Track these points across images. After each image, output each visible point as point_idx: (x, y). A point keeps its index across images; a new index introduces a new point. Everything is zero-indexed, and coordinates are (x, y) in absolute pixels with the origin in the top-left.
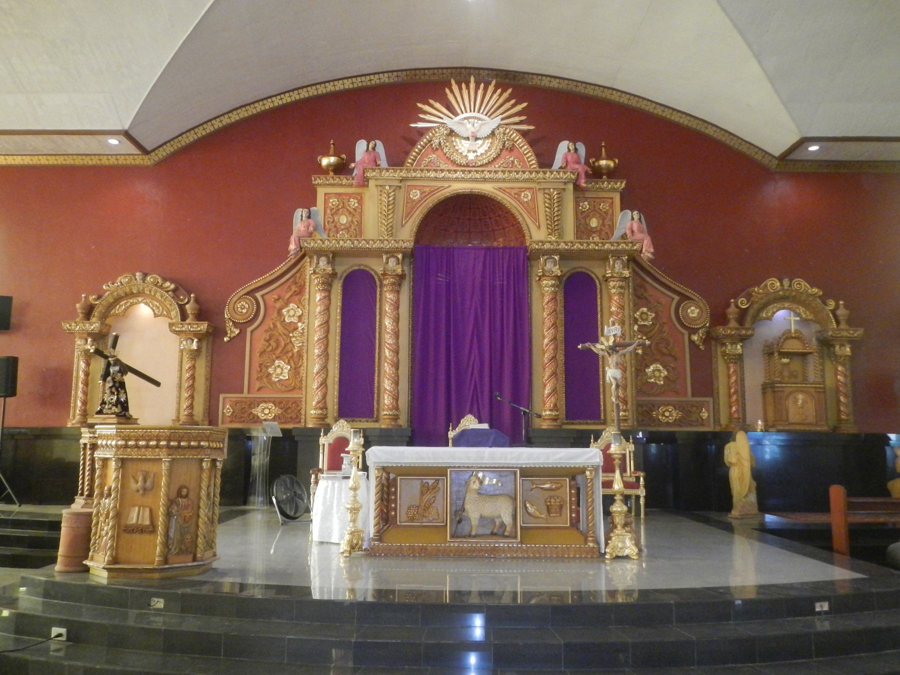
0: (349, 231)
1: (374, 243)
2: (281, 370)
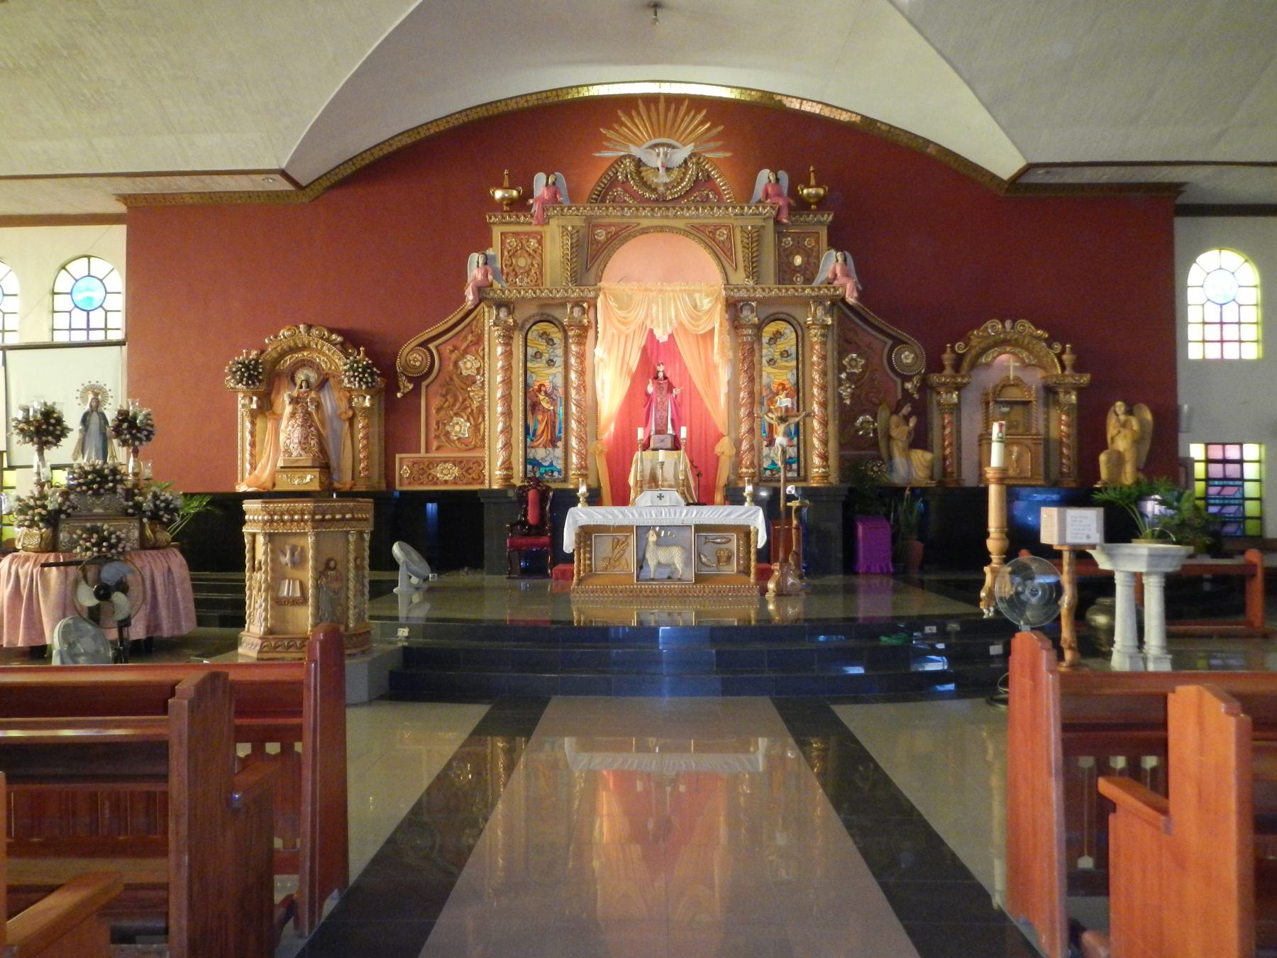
0: (528, 275)
2: (461, 427)
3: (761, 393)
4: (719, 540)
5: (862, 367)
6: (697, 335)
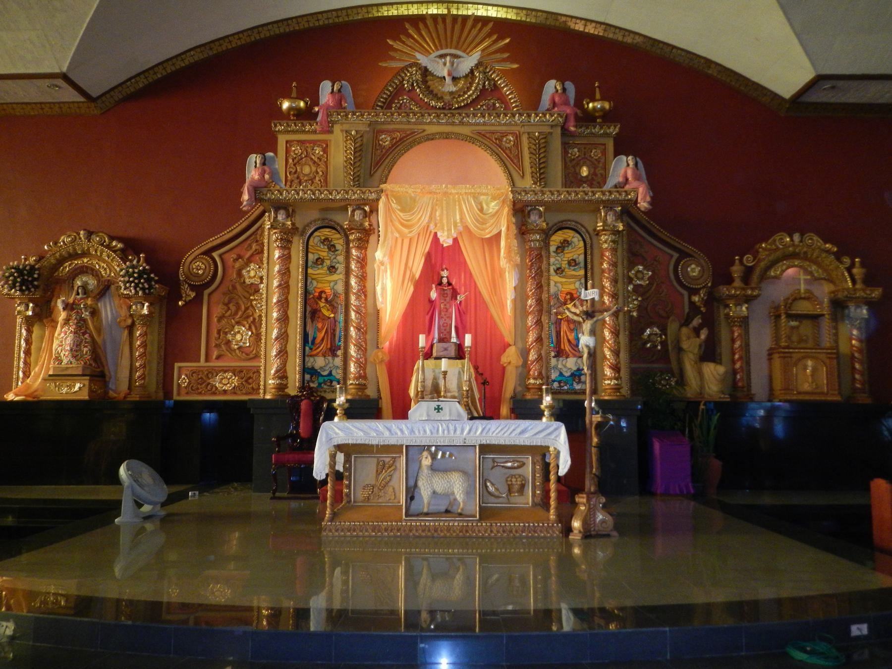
0: (313, 182)
1: (338, 193)
2: (242, 336)
3: (549, 302)
4: (509, 464)
5: (650, 278)
6: (482, 239)
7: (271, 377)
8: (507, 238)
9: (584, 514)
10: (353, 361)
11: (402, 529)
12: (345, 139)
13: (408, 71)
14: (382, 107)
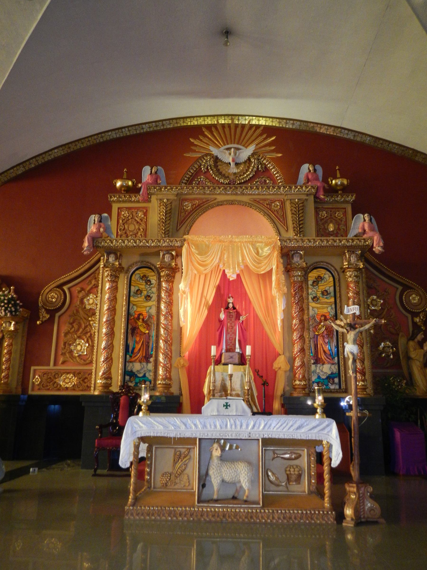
0: (136, 236)
1: (153, 242)
4: (287, 456)
5: (382, 305)
6: (258, 274)
7: (99, 377)
8: (277, 274)
9: (355, 503)
10: (161, 366)
11: (195, 514)
12: (159, 205)
13: (204, 159)
14: (186, 184)
